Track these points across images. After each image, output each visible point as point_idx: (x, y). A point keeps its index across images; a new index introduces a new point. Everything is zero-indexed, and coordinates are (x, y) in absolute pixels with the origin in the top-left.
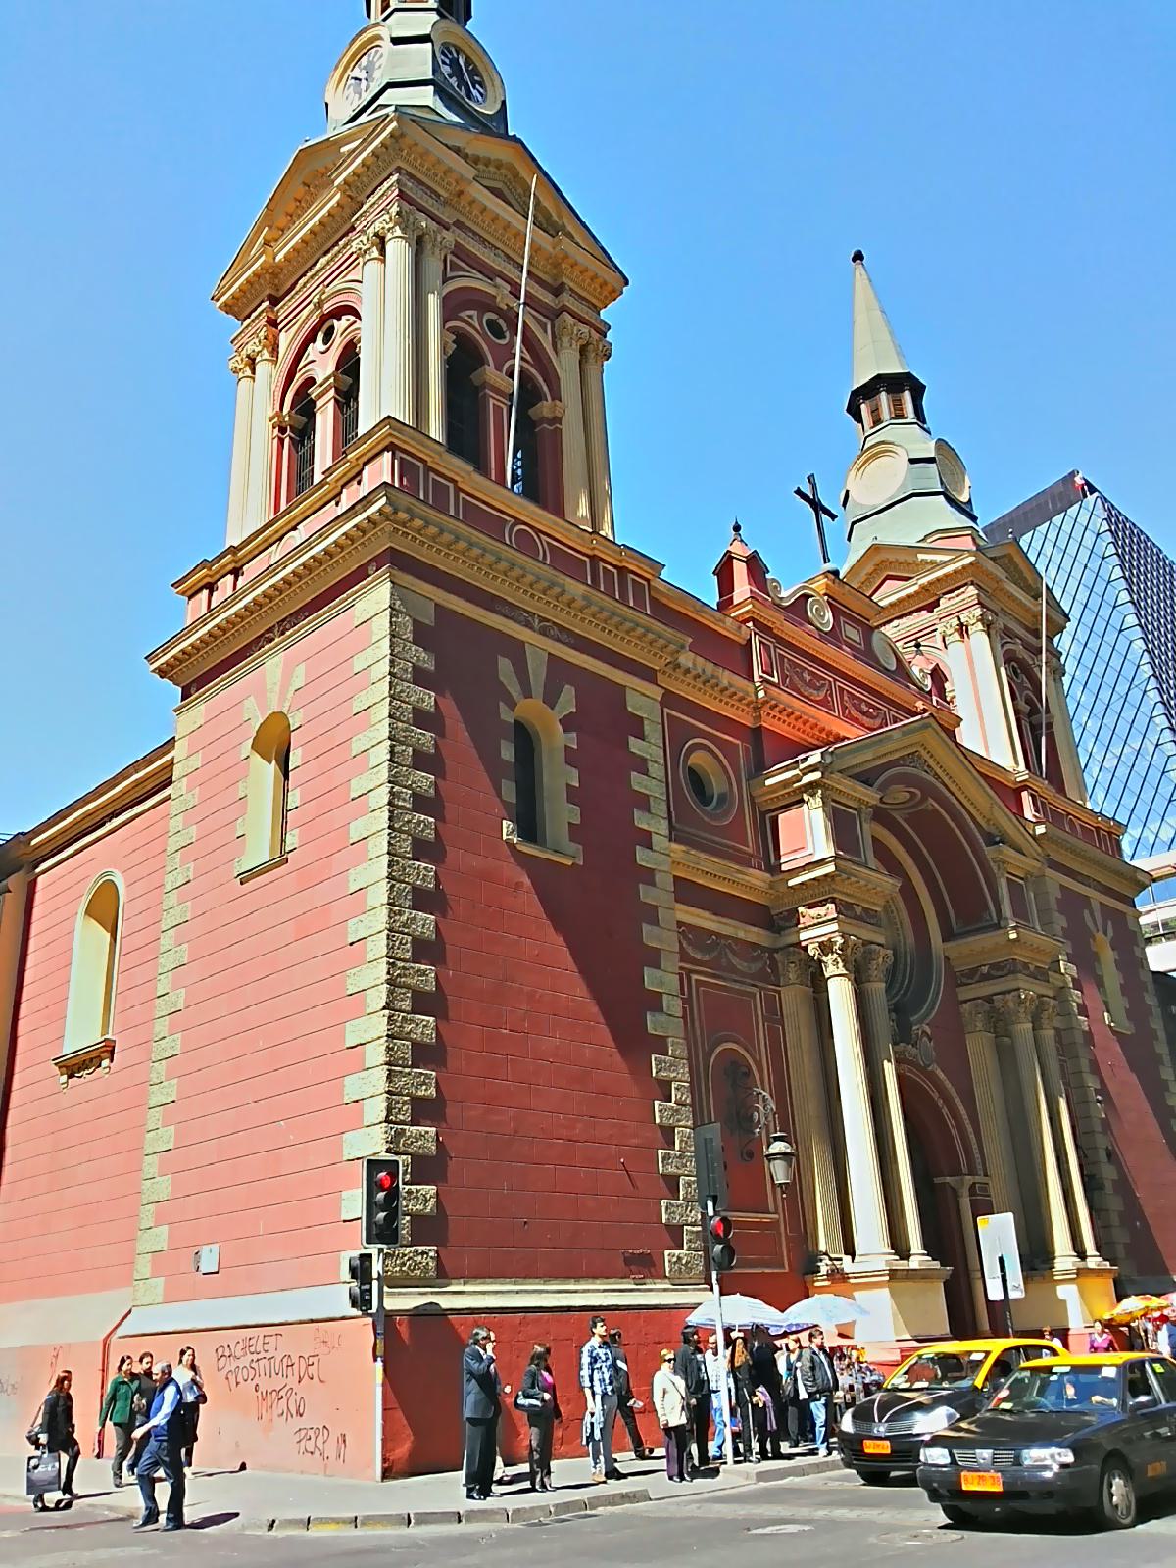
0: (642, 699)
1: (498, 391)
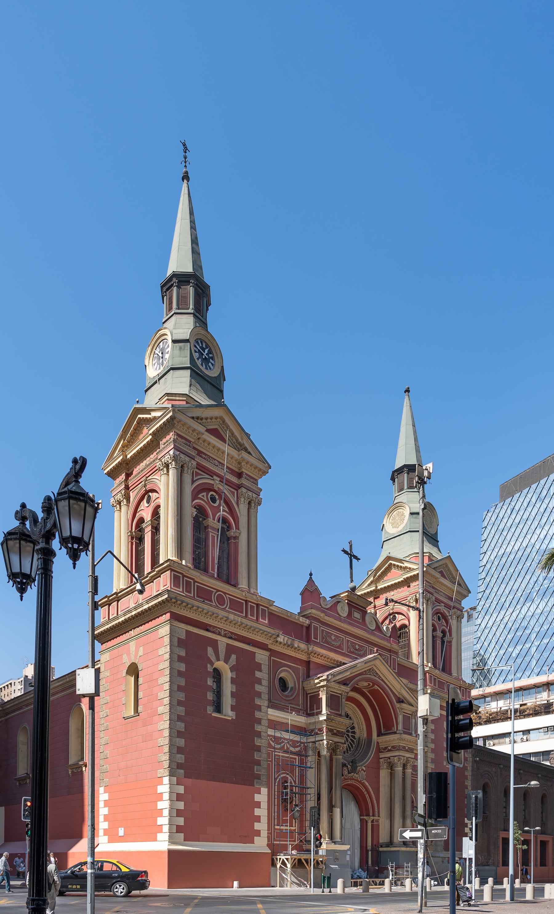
0: (261, 656)
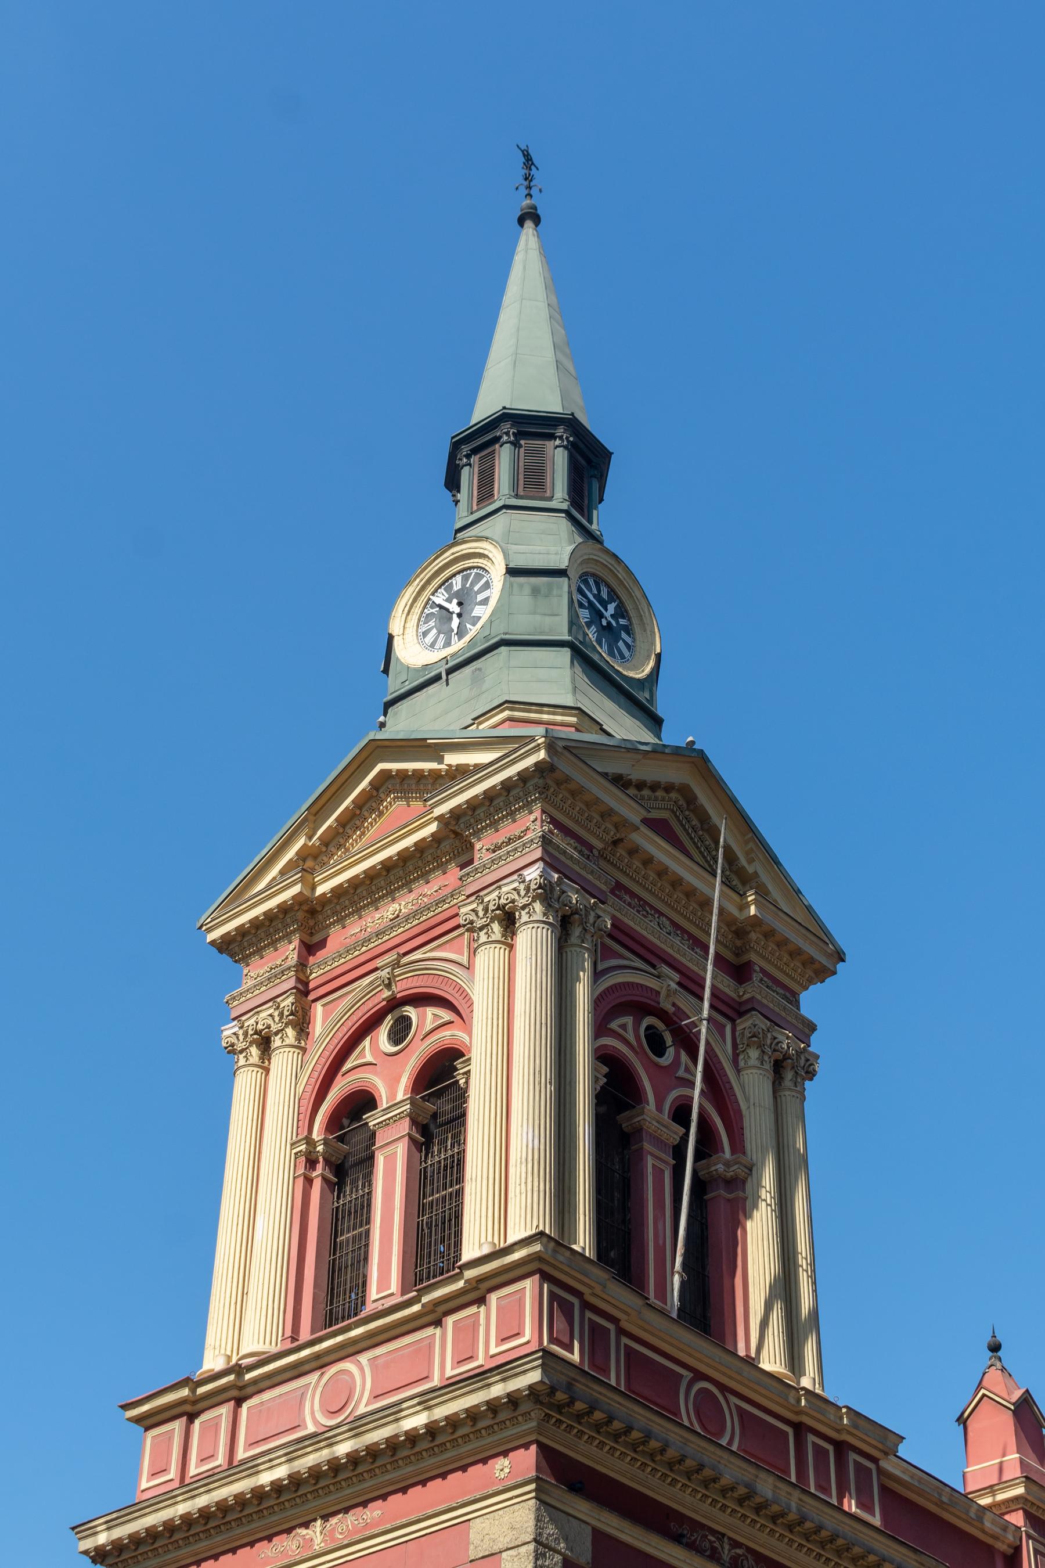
1: (659, 1142)
